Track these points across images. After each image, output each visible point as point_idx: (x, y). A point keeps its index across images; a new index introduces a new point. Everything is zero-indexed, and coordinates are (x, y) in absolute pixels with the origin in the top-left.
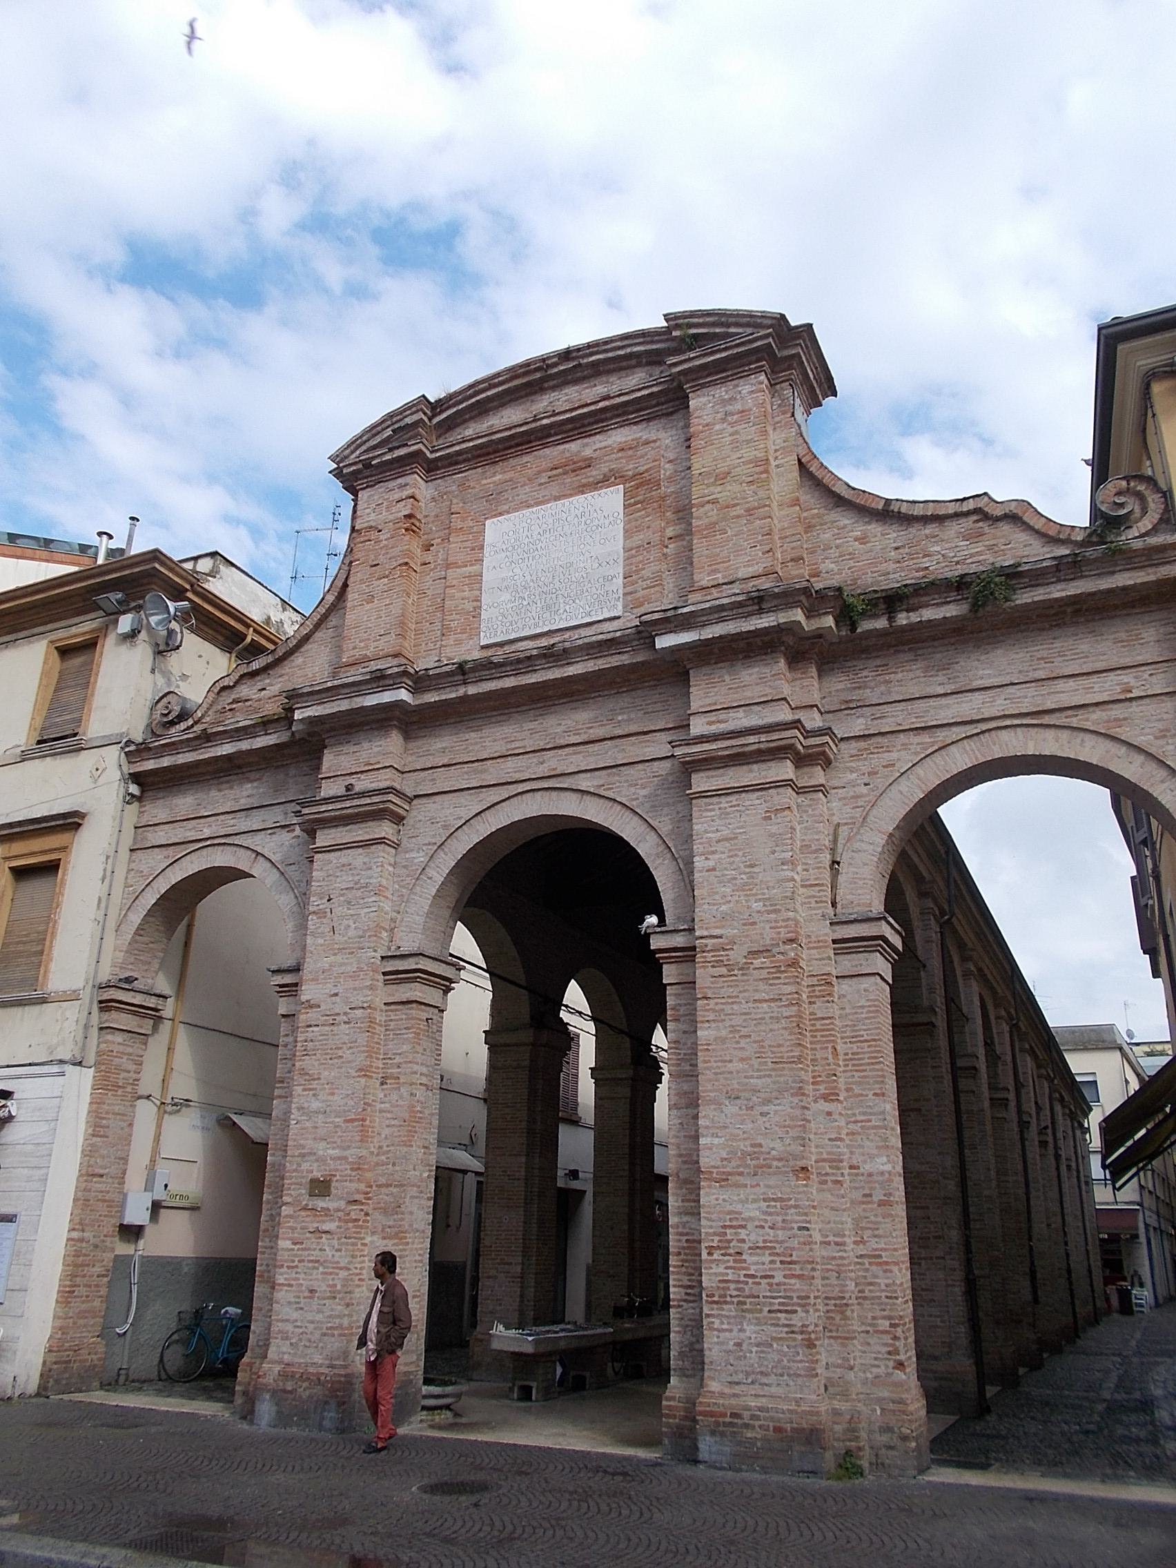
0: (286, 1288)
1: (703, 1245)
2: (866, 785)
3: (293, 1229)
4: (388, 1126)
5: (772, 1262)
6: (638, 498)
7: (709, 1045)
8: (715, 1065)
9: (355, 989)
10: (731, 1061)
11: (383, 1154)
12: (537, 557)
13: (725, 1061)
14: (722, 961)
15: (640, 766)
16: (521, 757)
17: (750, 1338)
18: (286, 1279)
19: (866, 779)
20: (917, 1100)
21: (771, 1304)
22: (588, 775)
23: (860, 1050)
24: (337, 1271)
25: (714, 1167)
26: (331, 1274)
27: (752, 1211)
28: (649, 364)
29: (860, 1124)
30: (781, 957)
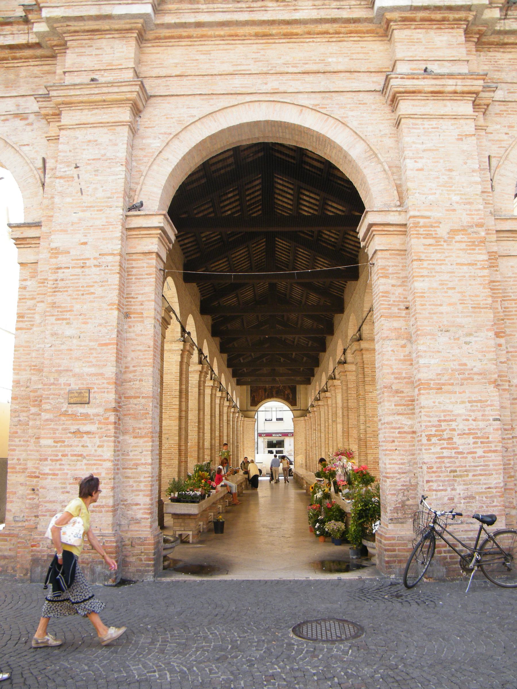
0: (51, 477)
1: (424, 434)
3: (54, 430)
4: (133, 351)
5: (475, 443)
7: (424, 293)
8: (429, 307)
9: (104, 239)
10: (441, 305)
11: (131, 372)
13: (437, 305)
14: (431, 234)
16: (247, 76)
17: (460, 494)
18: (50, 470)
19: (506, 130)
21: (475, 470)
22: (306, 96)
23: (509, 306)
24: (101, 462)
25: (431, 380)
26: (95, 464)
27: (460, 410)
29: (510, 354)
30: (475, 236)
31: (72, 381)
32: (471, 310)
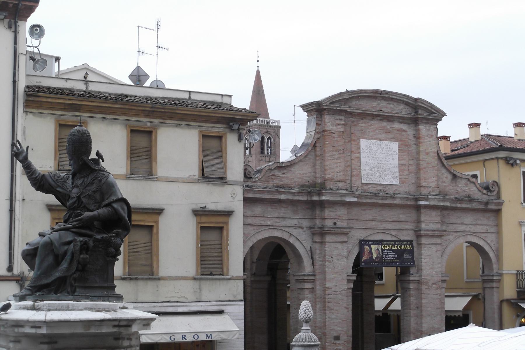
2: (445, 243)
6: (402, 149)
12: (376, 158)
15: (405, 231)
25: (425, 331)
28: (405, 104)
30: (438, 285)
31: (335, 332)
32: (436, 309)
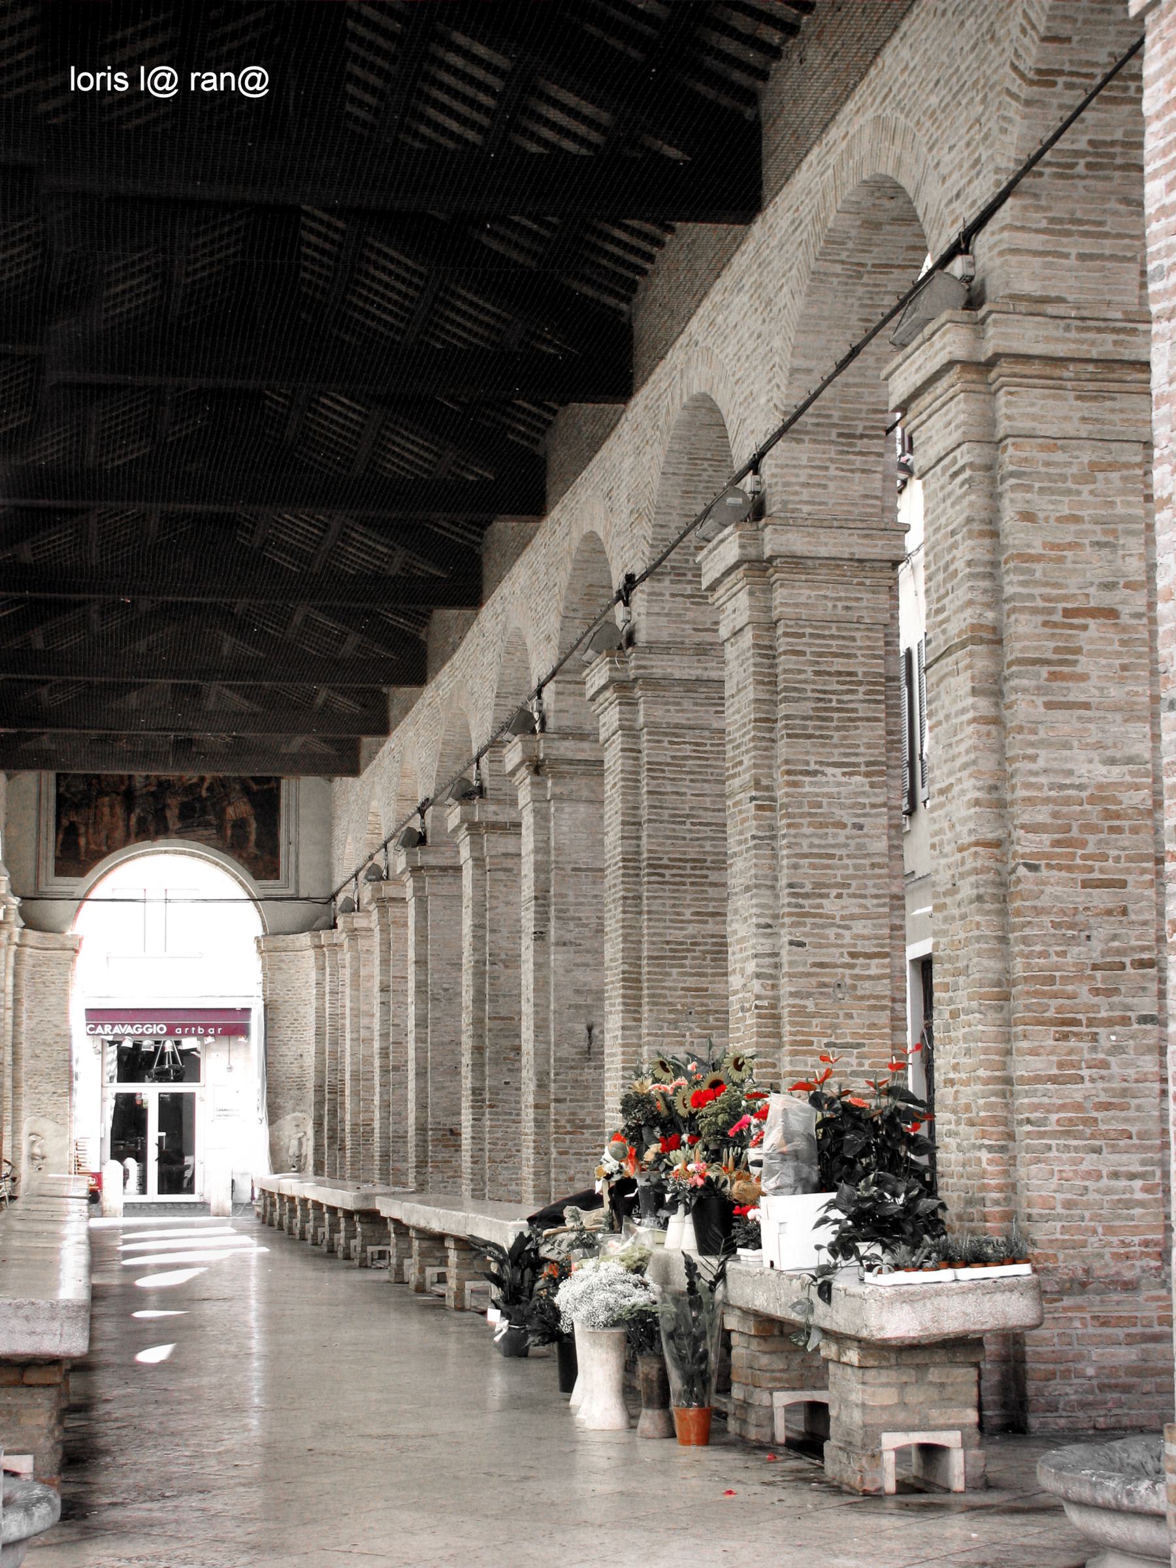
20: (1109, 586)
